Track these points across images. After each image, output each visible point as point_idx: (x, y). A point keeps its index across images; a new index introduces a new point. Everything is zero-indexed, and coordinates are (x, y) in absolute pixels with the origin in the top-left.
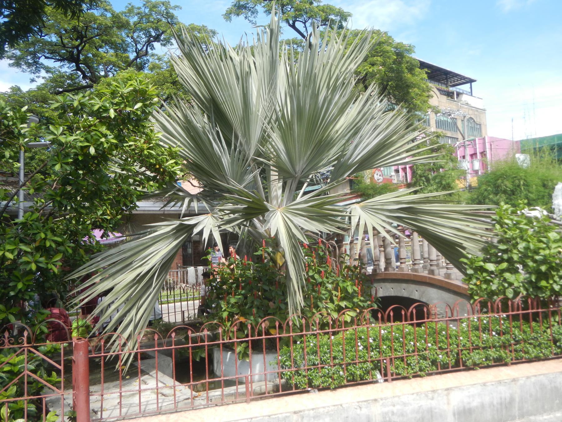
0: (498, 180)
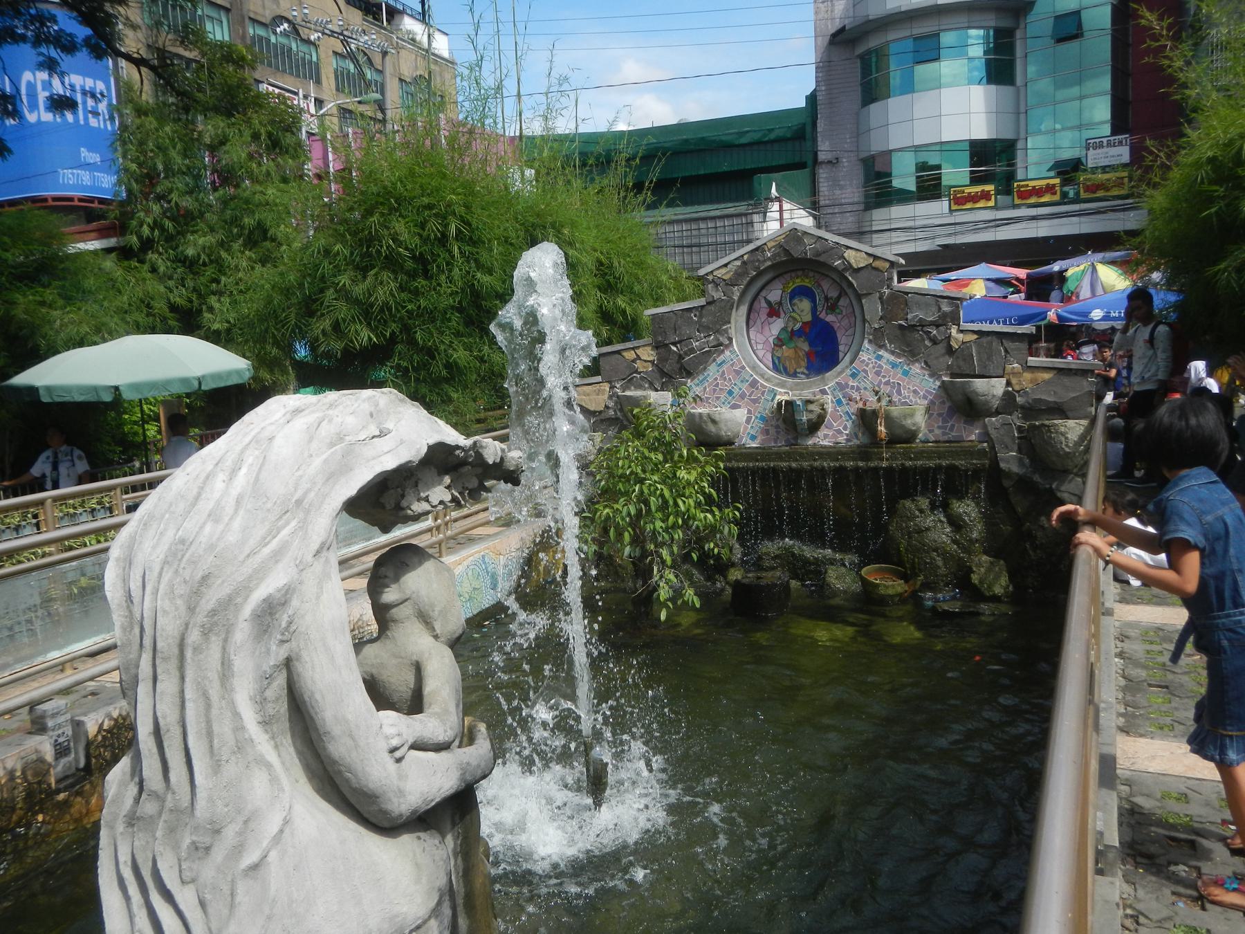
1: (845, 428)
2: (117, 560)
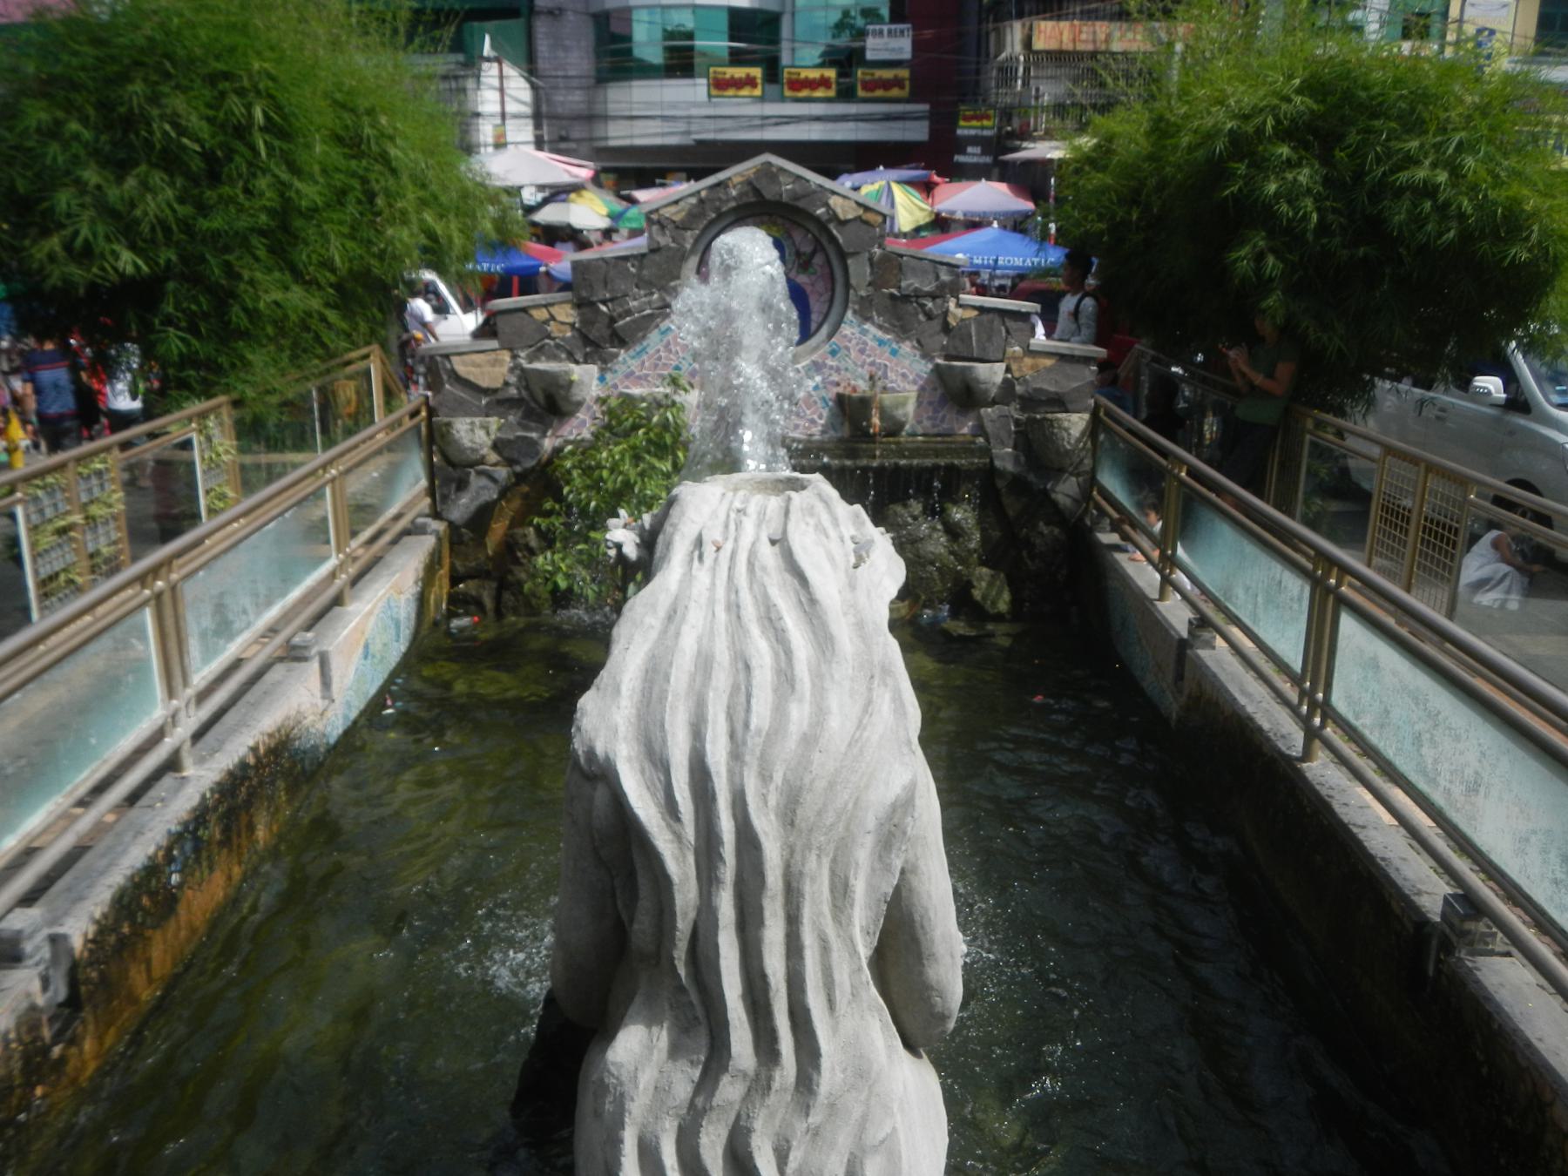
0: (124, 78)
1: (820, 417)
2: (629, 759)
